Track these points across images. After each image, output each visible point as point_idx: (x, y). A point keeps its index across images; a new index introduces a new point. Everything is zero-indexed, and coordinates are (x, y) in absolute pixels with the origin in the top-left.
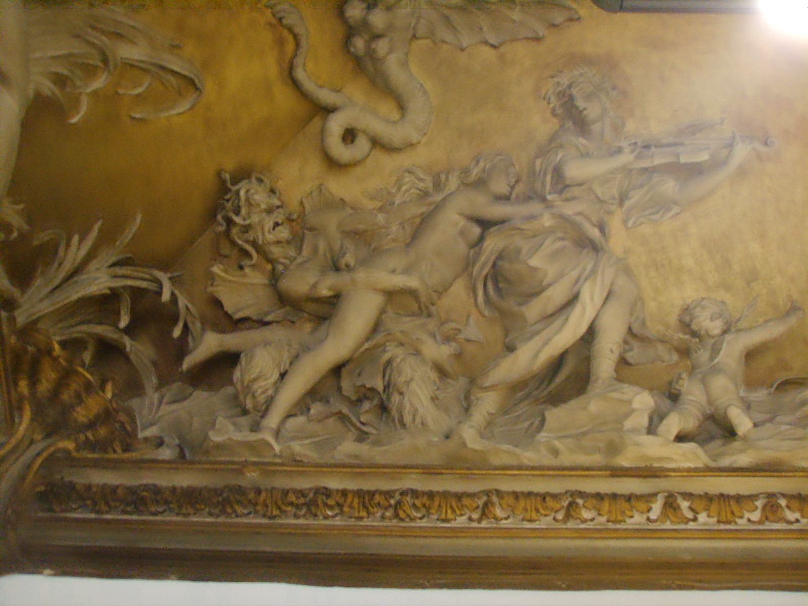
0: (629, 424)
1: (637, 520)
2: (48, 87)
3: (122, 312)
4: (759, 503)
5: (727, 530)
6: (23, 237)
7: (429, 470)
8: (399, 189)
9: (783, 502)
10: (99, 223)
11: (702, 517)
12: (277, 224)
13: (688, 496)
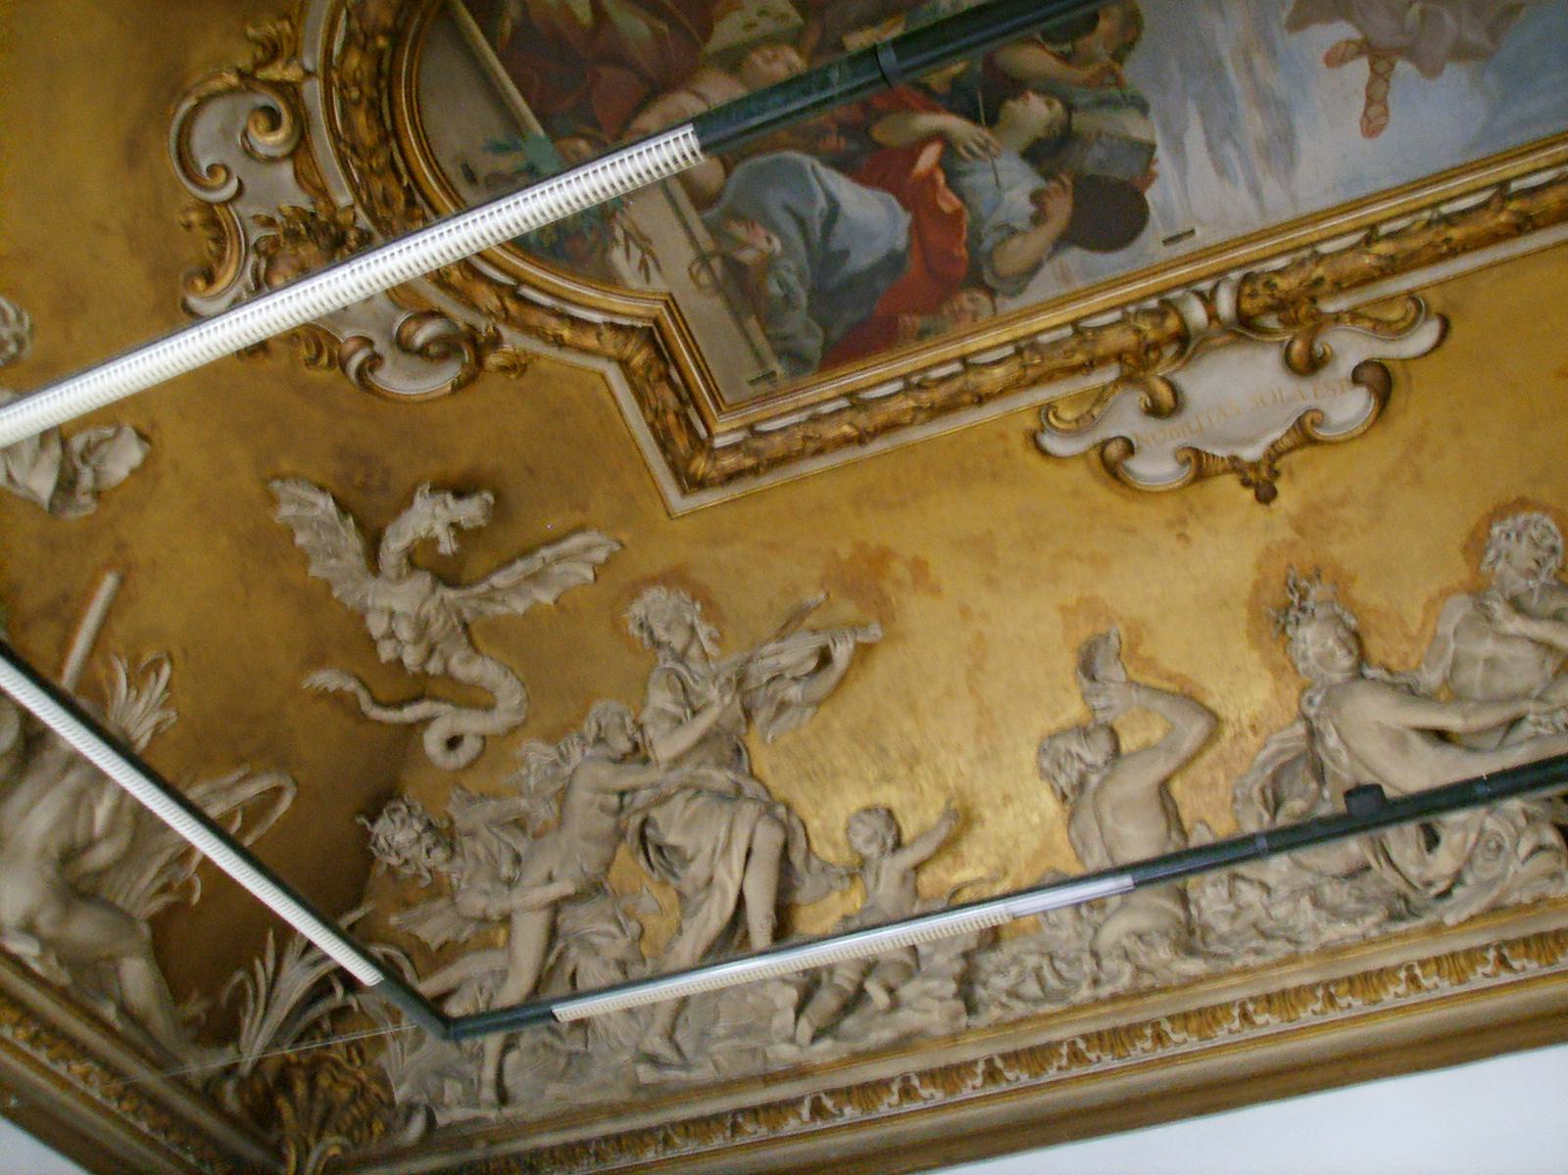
0: (777, 1023)
1: (792, 1125)
2: (156, 905)
3: (335, 985)
4: (895, 1088)
6: (209, 1012)
7: (615, 1111)
8: (528, 768)
9: (915, 1082)
10: (271, 935)
11: (848, 1110)
12: (428, 851)
13: (831, 1093)
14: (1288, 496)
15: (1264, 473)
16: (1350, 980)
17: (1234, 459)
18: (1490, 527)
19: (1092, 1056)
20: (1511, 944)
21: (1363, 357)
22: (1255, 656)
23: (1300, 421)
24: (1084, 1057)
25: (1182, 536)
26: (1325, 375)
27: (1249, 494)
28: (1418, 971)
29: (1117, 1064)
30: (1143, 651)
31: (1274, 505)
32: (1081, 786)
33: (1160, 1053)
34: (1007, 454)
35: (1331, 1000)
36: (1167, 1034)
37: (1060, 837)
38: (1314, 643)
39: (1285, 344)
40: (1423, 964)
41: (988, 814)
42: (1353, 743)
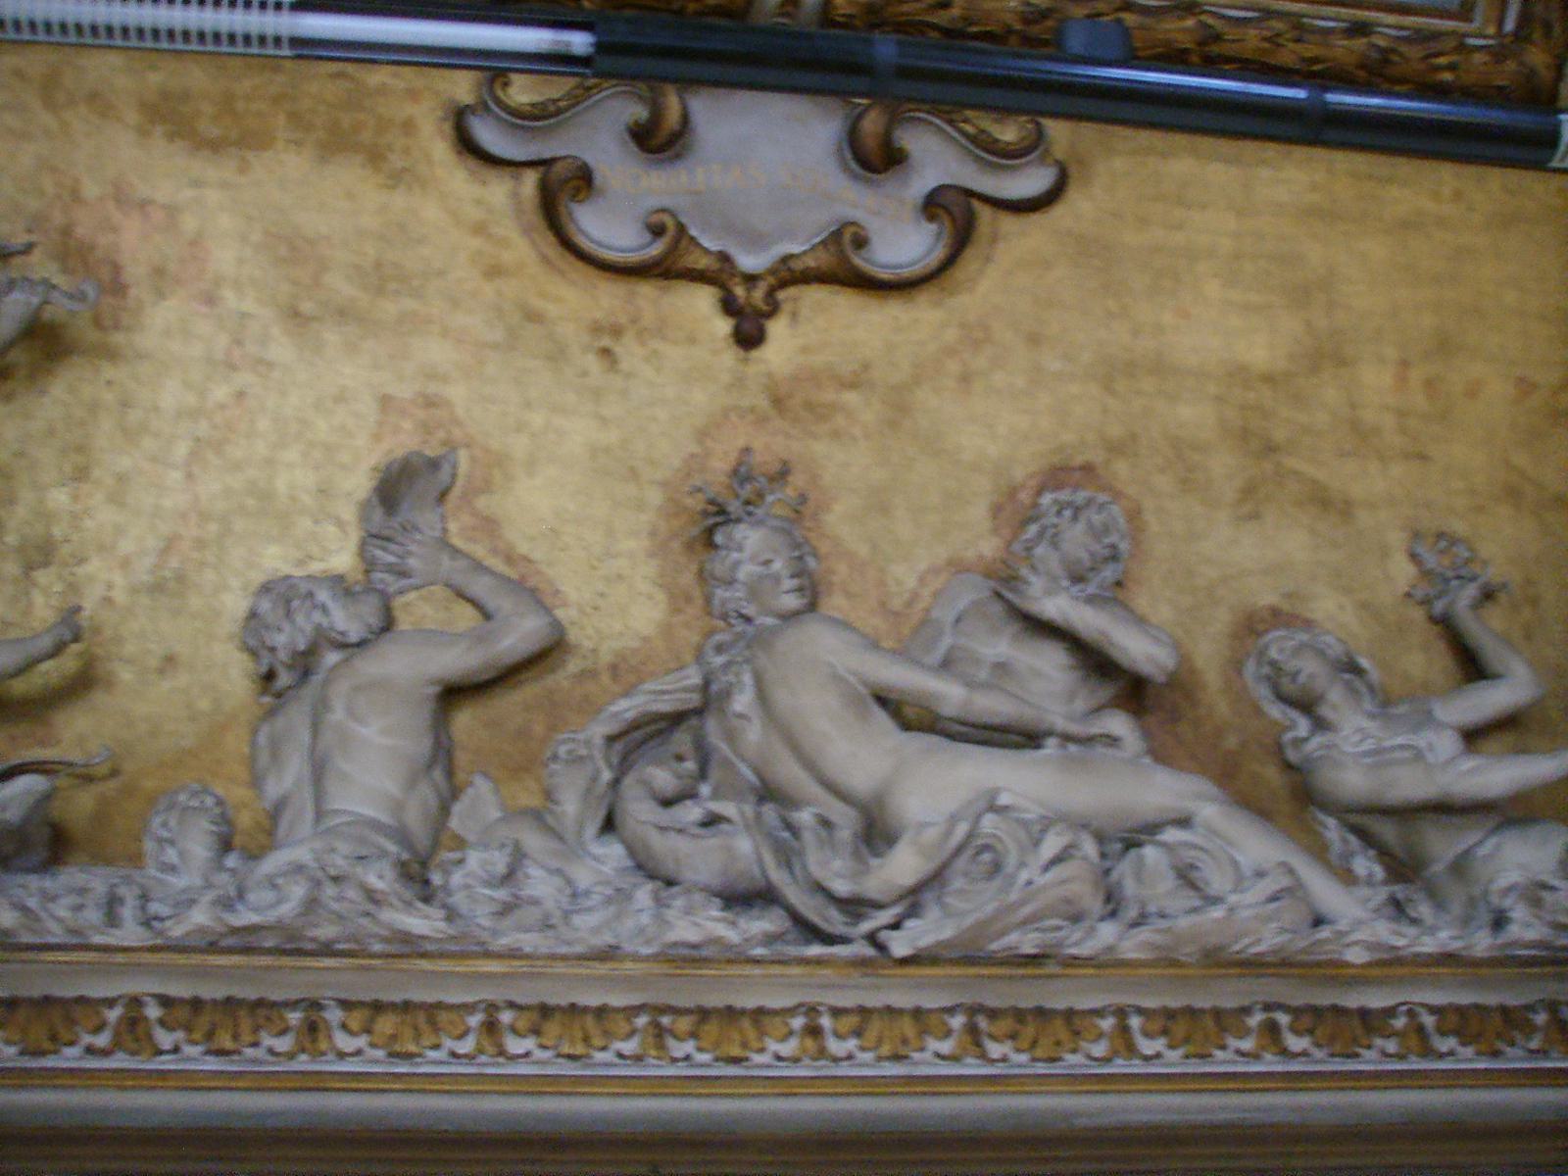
5: (959, 1078)
14: (782, 338)
15: (758, 294)
16: (704, 1014)
17: (724, 258)
18: (1039, 493)
19: (165, 1039)
20: (993, 1014)
21: (948, 181)
22: (649, 568)
23: (837, 235)
24: (150, 1037)
25: (606, 352)
26: (889, 182)
27: (724, 326)
28: (826, 1022)
29: (213, 1064)
30: (481, 502)
31: (755, 354)
32: (305, 663)
33: (303, 1063)
34: (409, 127)
35: (659, 1033)
36: (329, 1028)
37: (236, 742)
38: (752, 559)
39: (858, 110)
40: (837, 1012)
41: (126, 675)
42: (781, 697)
